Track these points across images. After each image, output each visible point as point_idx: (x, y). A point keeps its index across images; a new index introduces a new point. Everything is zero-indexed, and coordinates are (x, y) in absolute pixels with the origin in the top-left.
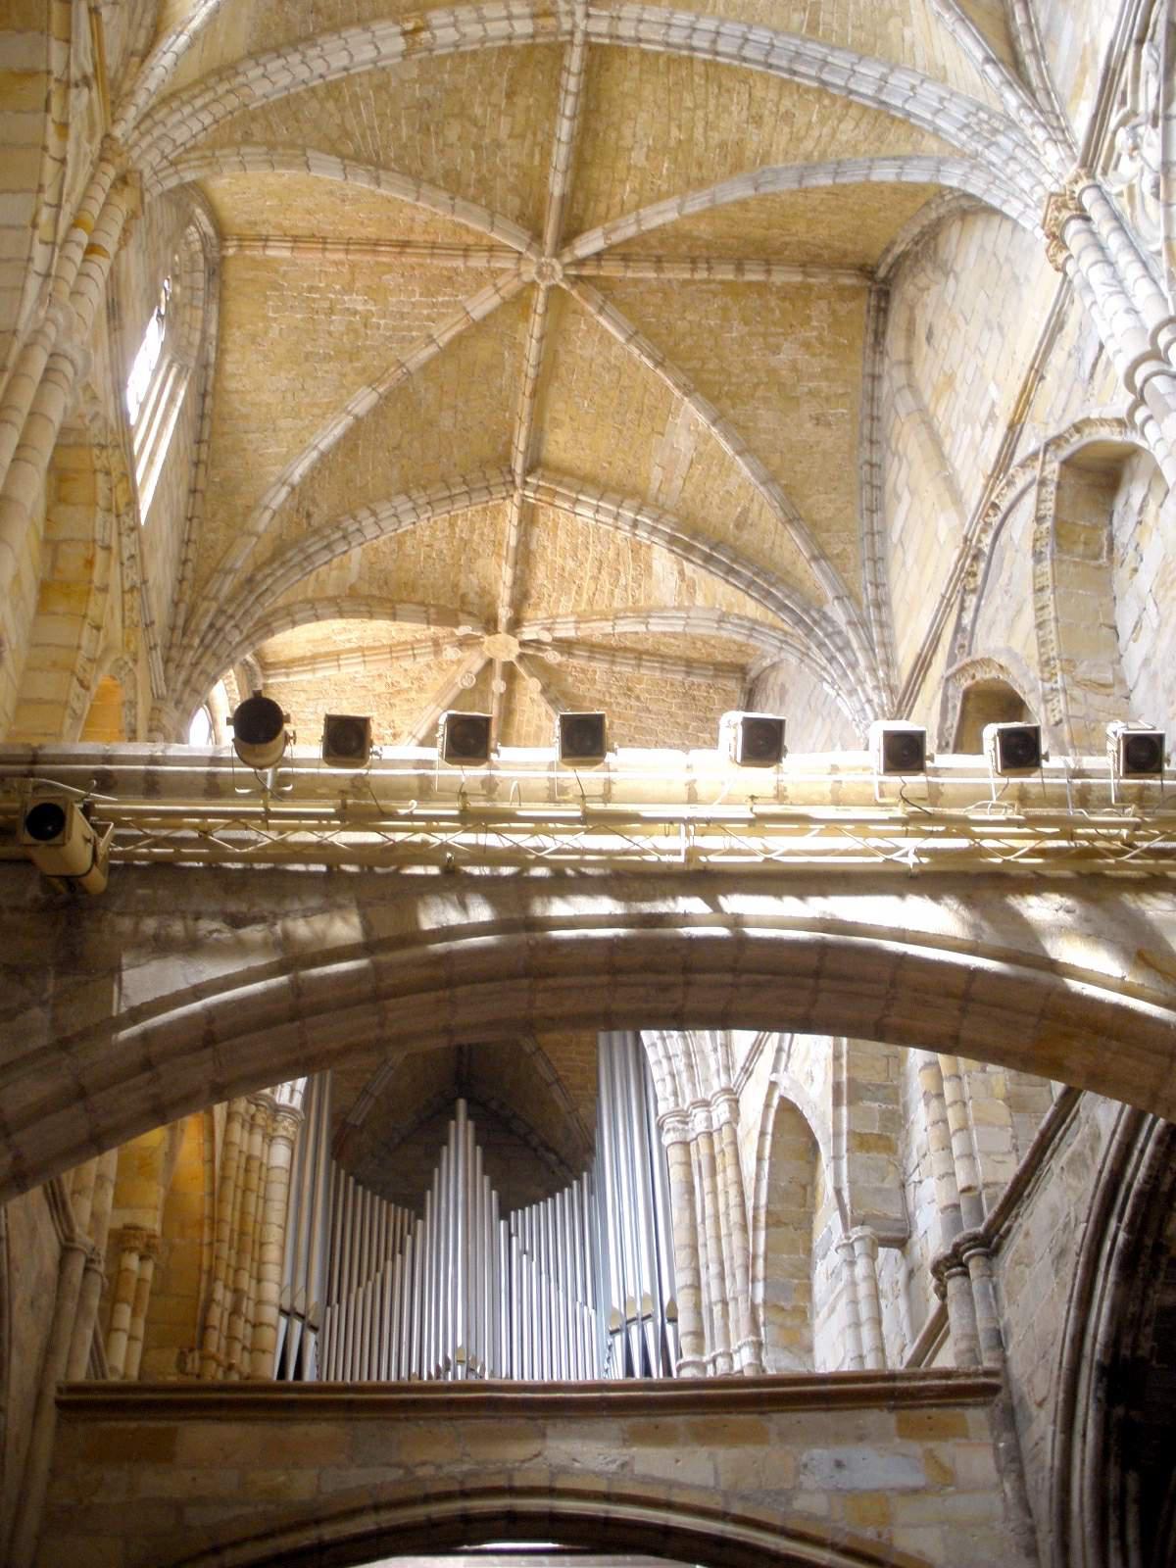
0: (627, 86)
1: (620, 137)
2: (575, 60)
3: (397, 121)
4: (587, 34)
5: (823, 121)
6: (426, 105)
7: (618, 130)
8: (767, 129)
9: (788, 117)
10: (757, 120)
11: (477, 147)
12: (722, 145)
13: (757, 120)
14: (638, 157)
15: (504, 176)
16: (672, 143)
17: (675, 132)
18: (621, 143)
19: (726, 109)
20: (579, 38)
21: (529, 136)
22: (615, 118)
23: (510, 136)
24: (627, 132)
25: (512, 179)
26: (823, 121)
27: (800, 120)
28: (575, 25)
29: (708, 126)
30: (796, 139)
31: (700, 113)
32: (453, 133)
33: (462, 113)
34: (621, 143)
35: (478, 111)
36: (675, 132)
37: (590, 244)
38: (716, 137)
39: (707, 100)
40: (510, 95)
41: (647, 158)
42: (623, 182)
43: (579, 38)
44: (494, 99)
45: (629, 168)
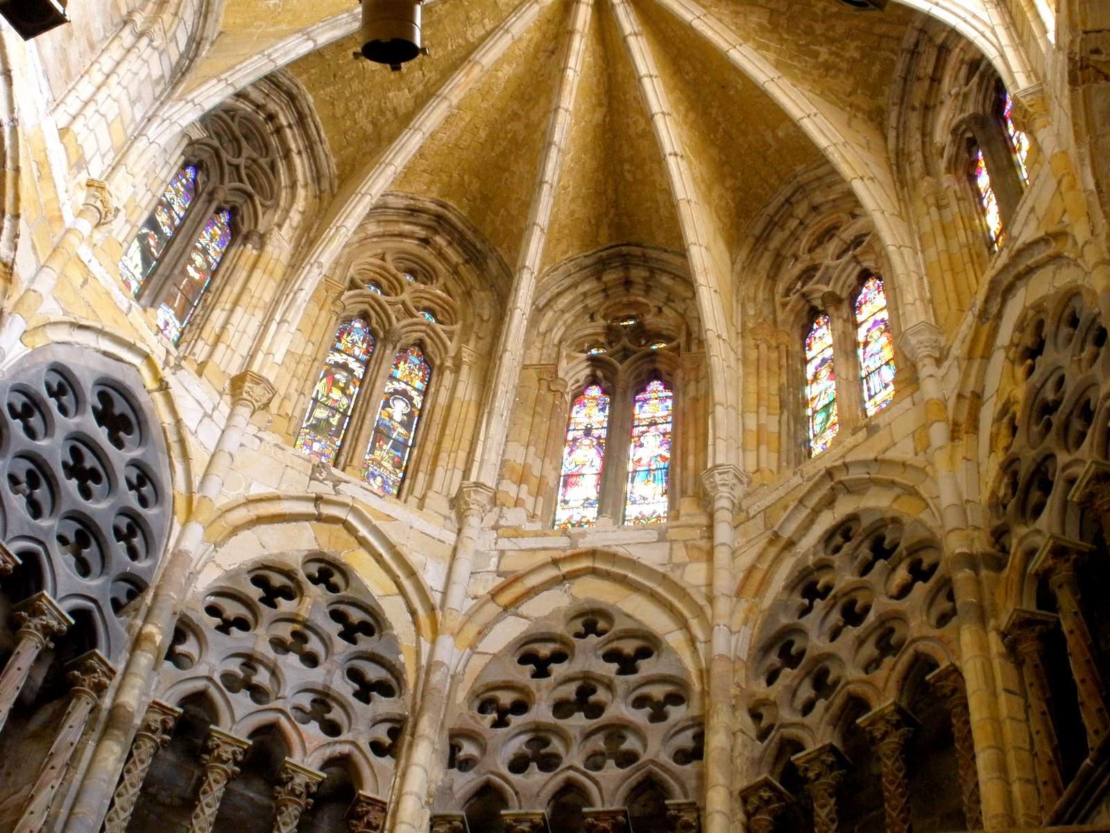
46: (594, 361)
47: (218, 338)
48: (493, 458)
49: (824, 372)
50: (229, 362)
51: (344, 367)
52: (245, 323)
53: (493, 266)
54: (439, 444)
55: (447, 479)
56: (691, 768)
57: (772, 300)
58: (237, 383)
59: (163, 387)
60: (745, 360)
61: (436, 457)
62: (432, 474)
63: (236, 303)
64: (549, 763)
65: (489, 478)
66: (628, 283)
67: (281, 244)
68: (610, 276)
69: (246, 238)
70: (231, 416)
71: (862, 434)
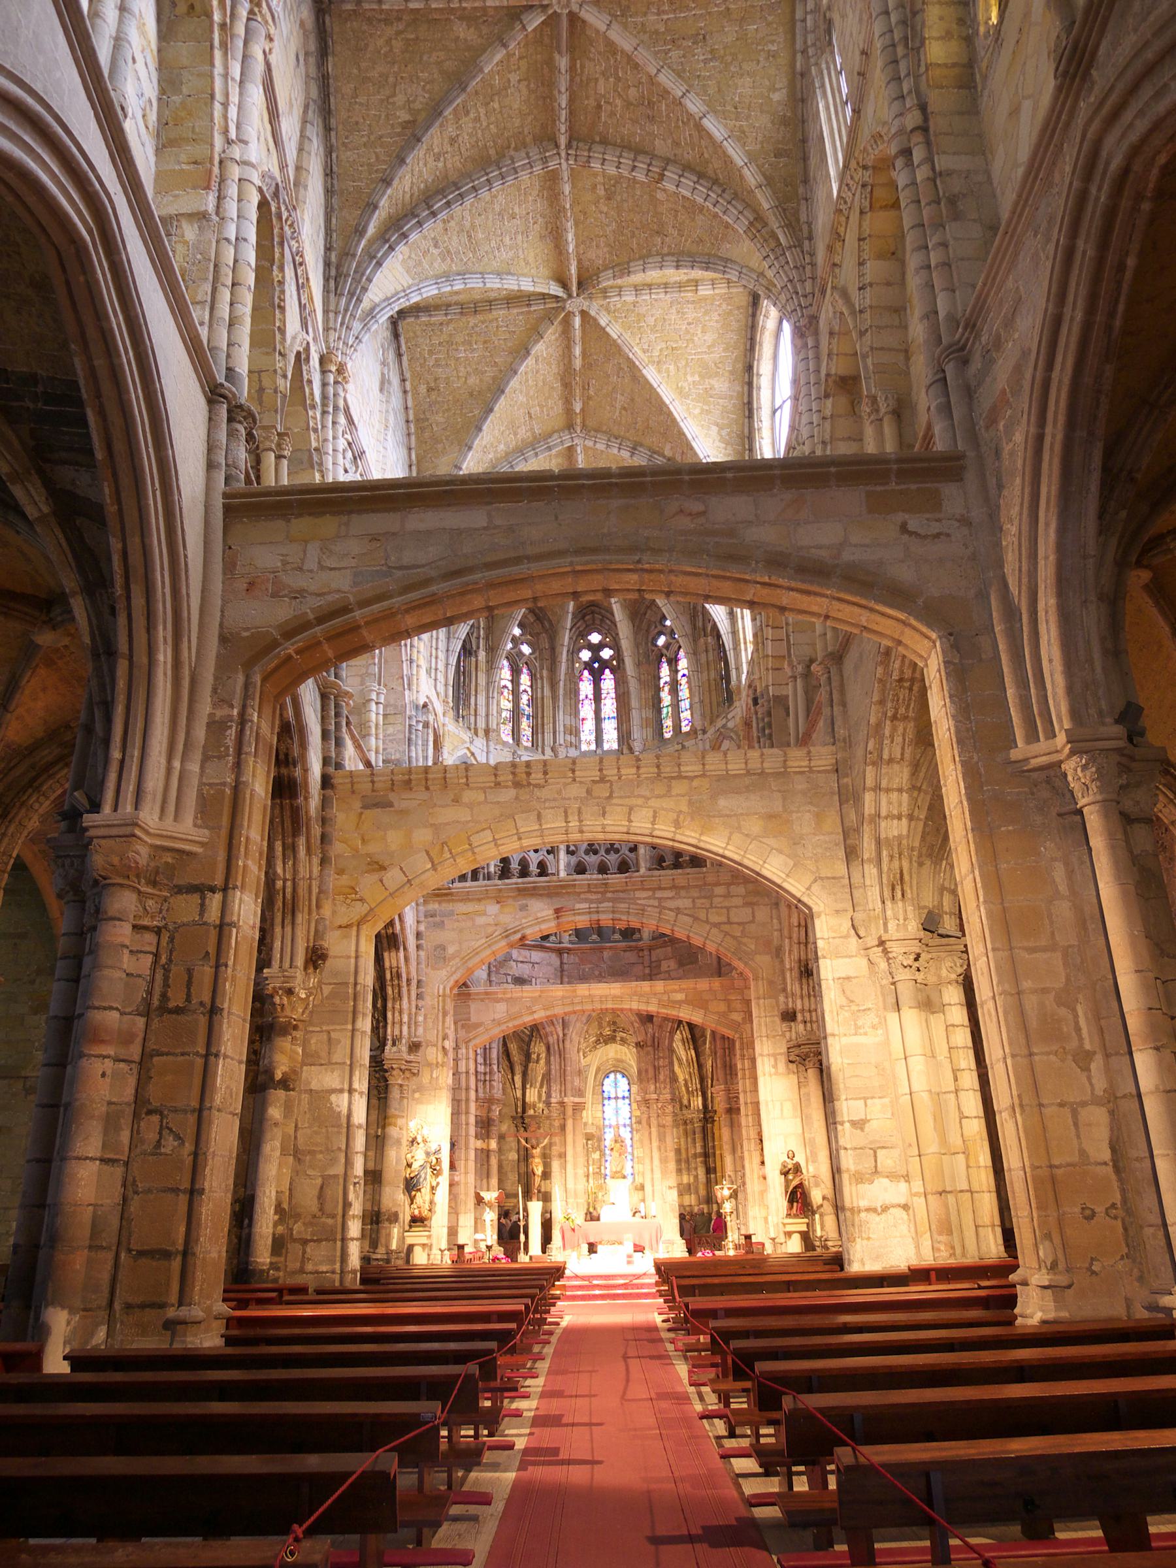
0: (530, 118)
1: (528, 86)
2: (563, 141)
3: (668, 116)
4: (559, 154)
5: (420, 172)
6: (651, 119)
7: (530, 91)
8: (446, 140)
9: (437, 159)
10: (453, 141)
11: (618, 79)
12: (467, 113)
13: (453, 141)
14: (514, 78)
15: (600, 53)
16: (496, 98)
17: (496, 105)
18: (526, 83)
19: (470, 135)
20: (563, 154)
21: (584, 79)
22: (533, 96)
23: (597, 80)
24: (525, 92)
25: (593, 50)
26: (420, 172)
27: (431, 163)
28: (567, 160)
29: (477, 119)
30: (430, 149)
31: (485, 124)
32: (633, 93)
33: (628, 104)
34: (526, 83)
35: (618, 102)
36: (496, 105)
37: (534, 21)
38: (472, 115)
39: (483, 135)
40: (599, 107)
41: (509, 80)
42: (521, 58)
43: (563, 154)
44: (609, 108)
45: (519, 68)
46: (585, 663)
47: (476, 711)
48: (562, 729)
49: (667, 689)
50: (481, 724)
51: (505, 687)
52: (482, 700)
53: (547, 624)
54: (543, 717)
55: (548, 738)
56: (632, 855)
57: (646, 644)
58: (487, 732)
59: (473, 754)
60: (639, 680)
61: (543, 725)
62: (543, 733)
63: (476, 691)
64: (596, 852)
65: (562, 742)
66: (594, 620)
67: (482, 655)
68: (587, 618)
69: (470, 654)
70: (488, 746)
71: (680, 746)
